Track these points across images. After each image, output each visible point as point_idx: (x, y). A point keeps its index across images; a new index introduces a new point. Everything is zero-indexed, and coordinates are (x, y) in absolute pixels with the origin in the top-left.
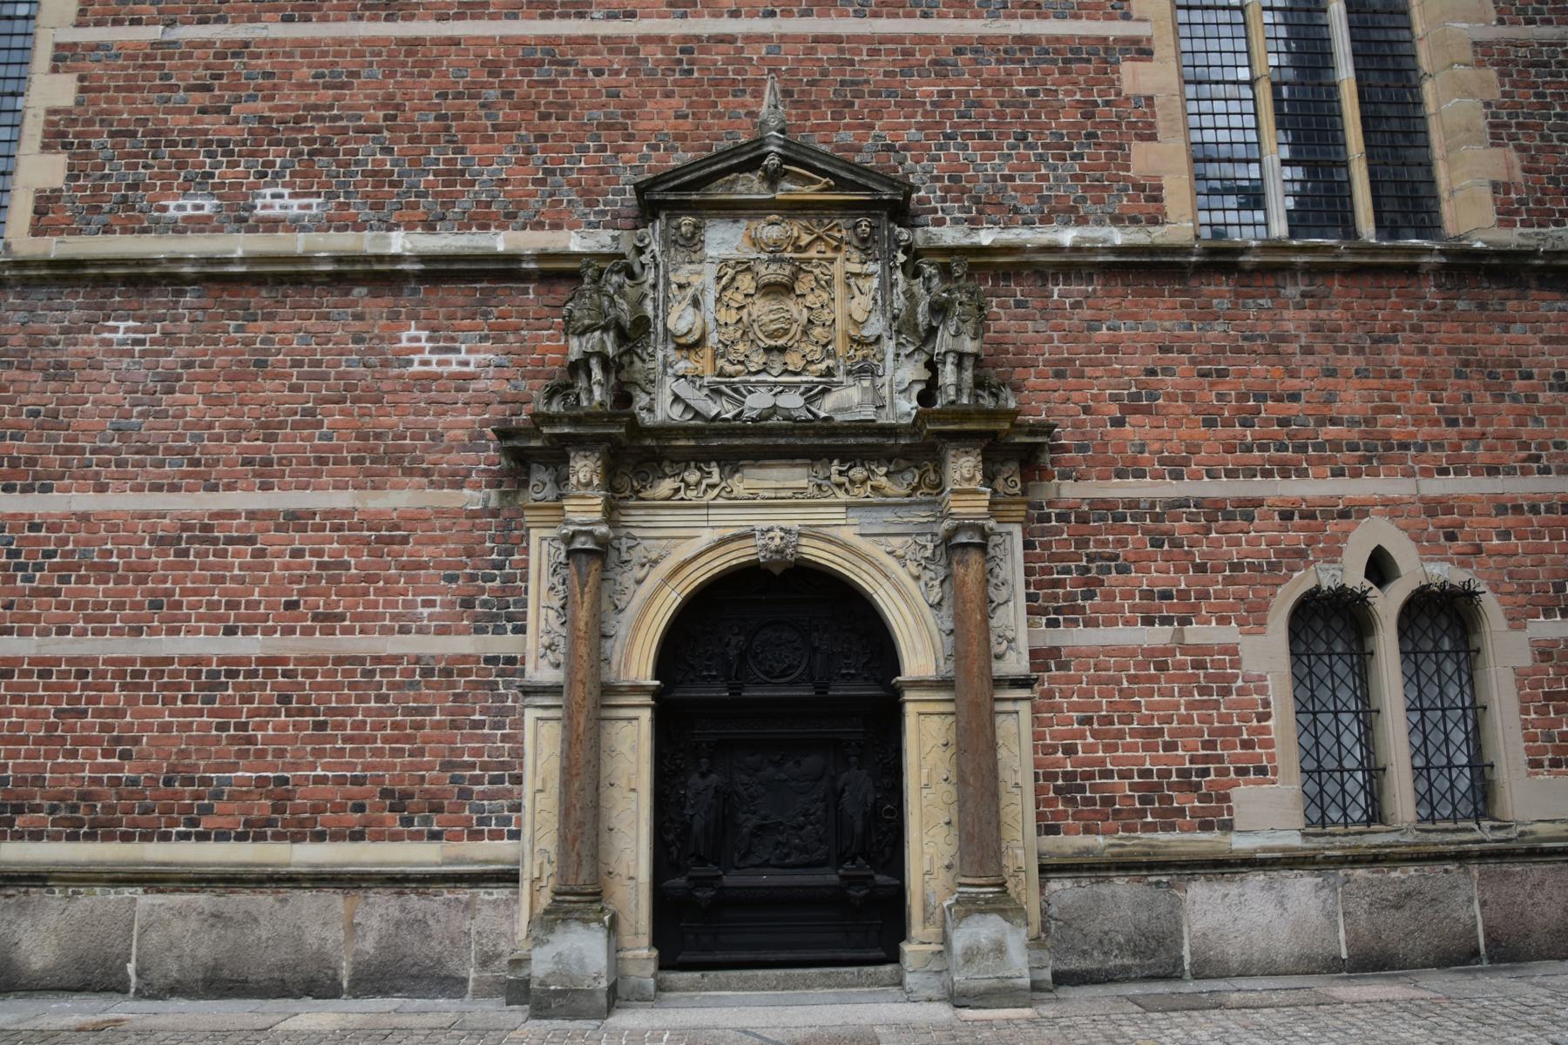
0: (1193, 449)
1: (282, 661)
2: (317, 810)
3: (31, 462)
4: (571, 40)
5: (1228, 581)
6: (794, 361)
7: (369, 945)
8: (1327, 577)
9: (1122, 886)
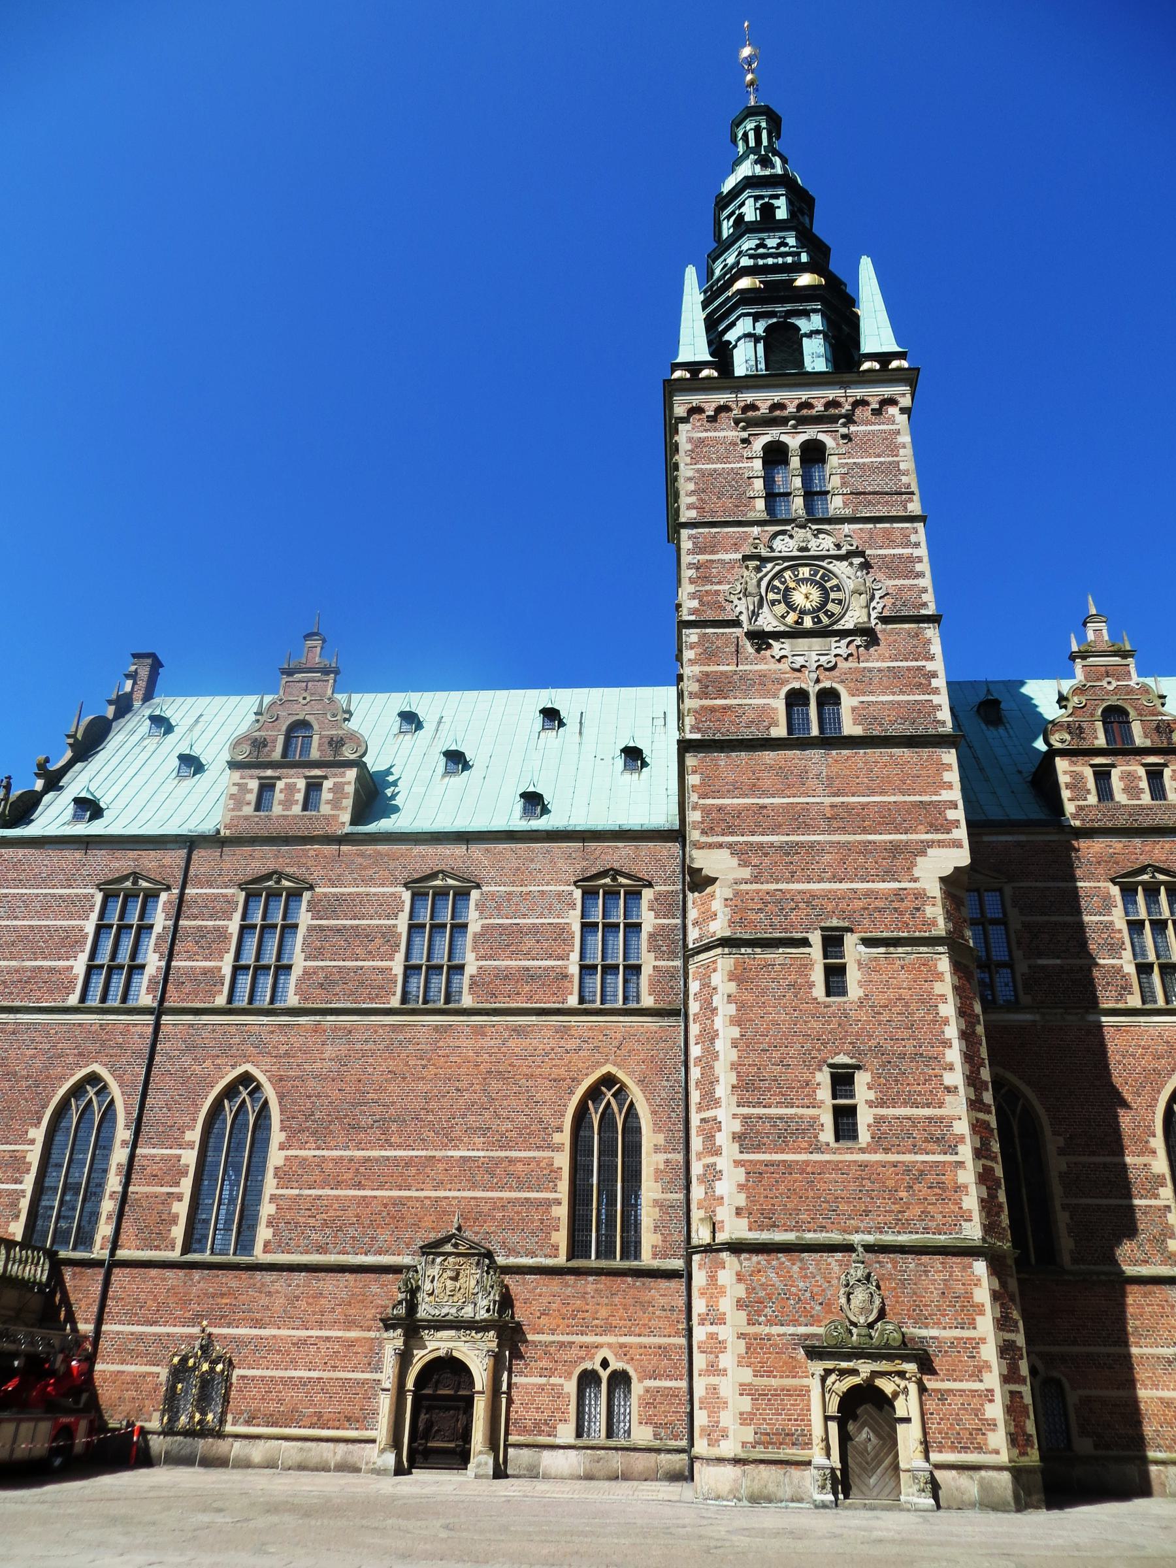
0: (558, 1326)
1: (322, 1378)
2: (328, 1420)
3: (261, 1320)
4: (406, 1197)
5: (563, 1365)
6: (455, 1299)
7: (338, 1458)
8: (588, 1365)
9: (525, 1451)
